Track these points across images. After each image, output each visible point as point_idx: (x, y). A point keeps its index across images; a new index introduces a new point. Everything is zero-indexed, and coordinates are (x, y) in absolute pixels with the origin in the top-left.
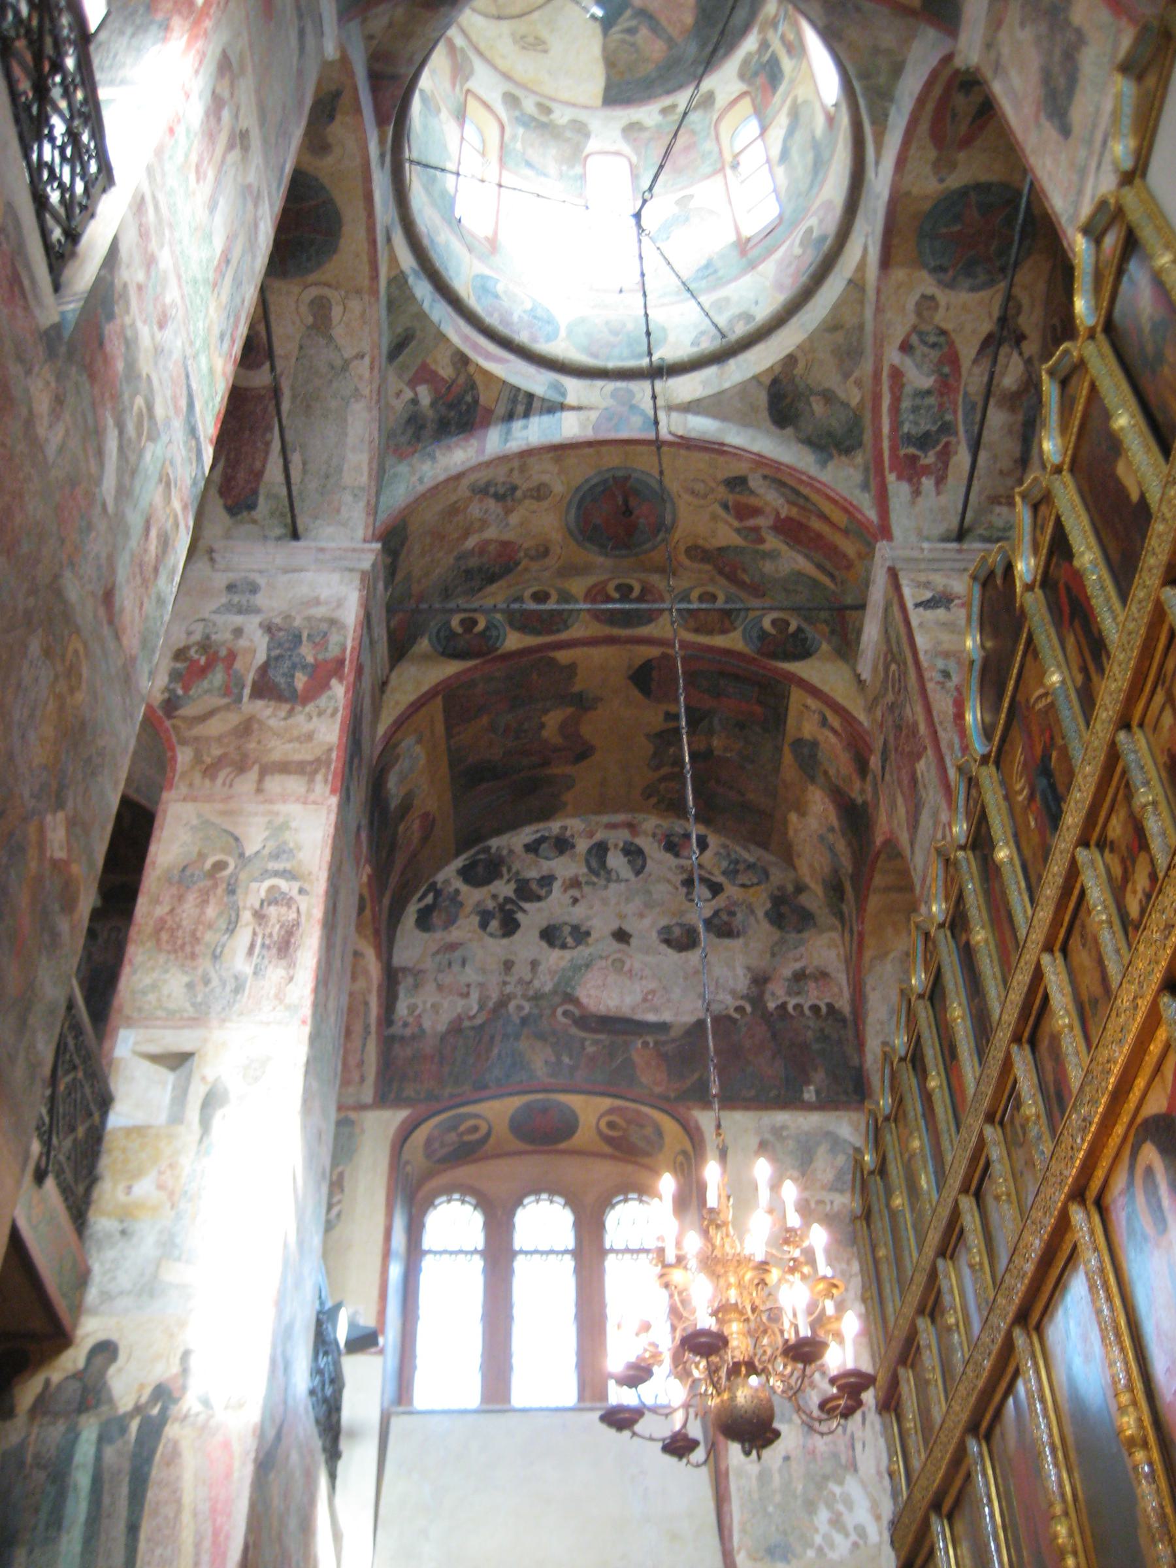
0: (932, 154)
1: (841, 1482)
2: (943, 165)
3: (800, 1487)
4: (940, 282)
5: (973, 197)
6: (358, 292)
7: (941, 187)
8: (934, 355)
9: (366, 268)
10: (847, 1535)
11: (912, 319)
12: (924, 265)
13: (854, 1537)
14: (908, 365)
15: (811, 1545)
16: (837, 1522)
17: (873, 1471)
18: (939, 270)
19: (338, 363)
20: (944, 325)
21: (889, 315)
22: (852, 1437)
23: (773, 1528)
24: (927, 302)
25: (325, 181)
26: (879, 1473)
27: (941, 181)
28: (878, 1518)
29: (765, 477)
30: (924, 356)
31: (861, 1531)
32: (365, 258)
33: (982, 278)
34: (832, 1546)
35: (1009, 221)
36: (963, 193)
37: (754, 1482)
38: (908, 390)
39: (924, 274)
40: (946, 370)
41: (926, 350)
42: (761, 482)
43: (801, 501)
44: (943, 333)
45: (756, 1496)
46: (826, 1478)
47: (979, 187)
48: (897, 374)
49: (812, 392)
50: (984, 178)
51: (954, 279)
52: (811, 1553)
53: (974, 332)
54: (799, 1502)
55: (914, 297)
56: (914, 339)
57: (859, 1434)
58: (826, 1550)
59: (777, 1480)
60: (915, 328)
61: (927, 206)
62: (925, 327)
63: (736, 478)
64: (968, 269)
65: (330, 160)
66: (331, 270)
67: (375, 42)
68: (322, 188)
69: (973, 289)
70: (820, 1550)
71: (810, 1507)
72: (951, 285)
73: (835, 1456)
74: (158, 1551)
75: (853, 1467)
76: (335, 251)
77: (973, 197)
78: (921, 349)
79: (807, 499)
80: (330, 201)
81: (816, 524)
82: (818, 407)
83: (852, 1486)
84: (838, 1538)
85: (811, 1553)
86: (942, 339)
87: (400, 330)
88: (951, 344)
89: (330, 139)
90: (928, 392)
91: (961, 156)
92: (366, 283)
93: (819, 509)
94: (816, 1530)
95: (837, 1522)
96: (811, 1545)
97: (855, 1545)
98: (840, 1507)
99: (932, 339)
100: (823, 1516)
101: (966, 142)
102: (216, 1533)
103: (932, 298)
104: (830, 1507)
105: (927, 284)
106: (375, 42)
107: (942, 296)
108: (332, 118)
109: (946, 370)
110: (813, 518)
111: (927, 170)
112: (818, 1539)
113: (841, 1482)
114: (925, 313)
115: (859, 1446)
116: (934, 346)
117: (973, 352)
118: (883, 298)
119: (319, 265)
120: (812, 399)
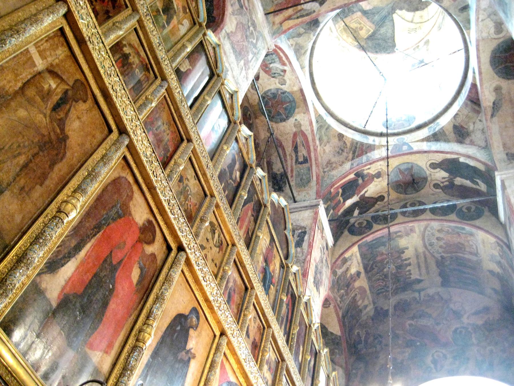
0: (303, 128)
2: (298, 125)
4: (281, 89)
5: (284, 117)
6: (483, 39)
7: (295, 118)
8: (273, 71)
9: (481, 48)
11: (286, 78)
12: (288, 93)
14: (282, 67)
18: (284, 93)
19: (492, 17)
20: (274, 79)
21: (294, 77)
24: (283, 83)
25: (496, 76)
27: (296, 120)
29: (314, 11)
30: (277, 70)
32: (481, 51)
33: (269, 94)
35: (269, 112)
36: (288, 118)
38: (278, 62)
39: (288, 91)
40: (267, 69)
41: (277, 72)
42: (314, 8)
43: (299, 14)
44: (273, 77)
47: (284, 120)
48: (284, 64)
49: (305, 33)
50: (284, 124)
51: (278, 91)
53: (264, 80)
55: (288, 82)
56: (282, 74)
60: (283, 76)
61: (297, 110)
62: (281, 77)
63: (323, 3)
64: (275, 95)
65: (494, 85)
66: (494, 45)
67: (479, 118)
68: (497, 74)
69: (270, 90)
72: (278, 90)
76: (493, 51)
77: (284, 117)
78: (279, 71)
79: (298, 18)
80: (494, 69)
81: (290, 11)
82: (302, 30)
86: (273, 75)
87: (465, 13)
88: (269, 75)
89: (494, 94)
90: (270, 63)
91: (294, 130)
92: (480, 43)
93: (291, 19)
99: (276, 75)
101: (295, 135)
103: (282, 85)
105: (285, 88)
106: (479, 118)
107: (279, 86)
108: (494, 103)
109: (267, 69)
110: (292, 13)
111: (302, 123)
114: (282, 80)
116: (275, 74)
117: (261, 75)
118: (298, 81)
119: (499, 45)
120: (304, 31)
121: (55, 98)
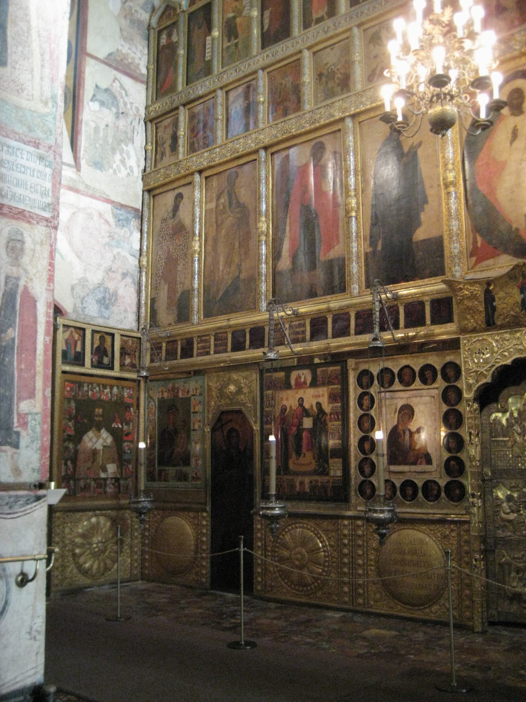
1: (127, 146)
3: (110, 141)
10: (126, 169)
13: (128, 171)
15: (112, 168)
16: (123, 161)
17: (139, 146)
22: (134, 128)
23: (98, 154)
26: (141, 147)
28: (139, 166)
31: (131, 168)
34: (120, 171)
37: (92, 130)
45: (92, 137)
46: (121, 141)
52: (111, 171)
54: (109, 147)
57: (136, 127)
58: (117, 172)
59: (101, 134)
70: (115, 171)
71: (114, 150)
73: (126, 133)
74: (20, 49)
75: (132, 141)
83: (130, 148)
84: (123, 169)
85: (111, 171)
94: (115, 162)
95: (123, 161)
96: (112, 168)
97: (129, 174)
98: (125, 155)
100: (118, 157)
102: (51, 53)
104: (121, 154)
112: (115, 166)
113: (127, 146)
115: (136, 132)
121: (227, 203)
